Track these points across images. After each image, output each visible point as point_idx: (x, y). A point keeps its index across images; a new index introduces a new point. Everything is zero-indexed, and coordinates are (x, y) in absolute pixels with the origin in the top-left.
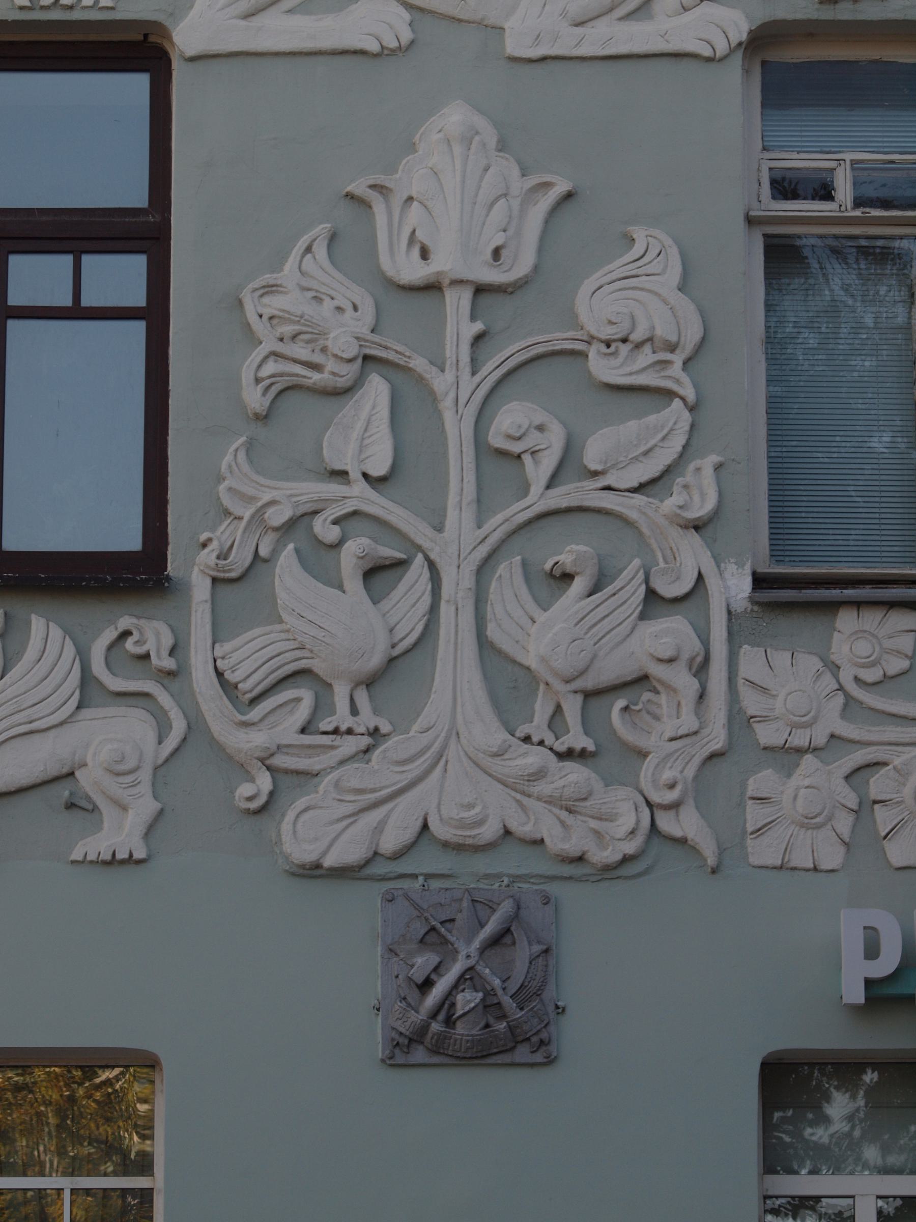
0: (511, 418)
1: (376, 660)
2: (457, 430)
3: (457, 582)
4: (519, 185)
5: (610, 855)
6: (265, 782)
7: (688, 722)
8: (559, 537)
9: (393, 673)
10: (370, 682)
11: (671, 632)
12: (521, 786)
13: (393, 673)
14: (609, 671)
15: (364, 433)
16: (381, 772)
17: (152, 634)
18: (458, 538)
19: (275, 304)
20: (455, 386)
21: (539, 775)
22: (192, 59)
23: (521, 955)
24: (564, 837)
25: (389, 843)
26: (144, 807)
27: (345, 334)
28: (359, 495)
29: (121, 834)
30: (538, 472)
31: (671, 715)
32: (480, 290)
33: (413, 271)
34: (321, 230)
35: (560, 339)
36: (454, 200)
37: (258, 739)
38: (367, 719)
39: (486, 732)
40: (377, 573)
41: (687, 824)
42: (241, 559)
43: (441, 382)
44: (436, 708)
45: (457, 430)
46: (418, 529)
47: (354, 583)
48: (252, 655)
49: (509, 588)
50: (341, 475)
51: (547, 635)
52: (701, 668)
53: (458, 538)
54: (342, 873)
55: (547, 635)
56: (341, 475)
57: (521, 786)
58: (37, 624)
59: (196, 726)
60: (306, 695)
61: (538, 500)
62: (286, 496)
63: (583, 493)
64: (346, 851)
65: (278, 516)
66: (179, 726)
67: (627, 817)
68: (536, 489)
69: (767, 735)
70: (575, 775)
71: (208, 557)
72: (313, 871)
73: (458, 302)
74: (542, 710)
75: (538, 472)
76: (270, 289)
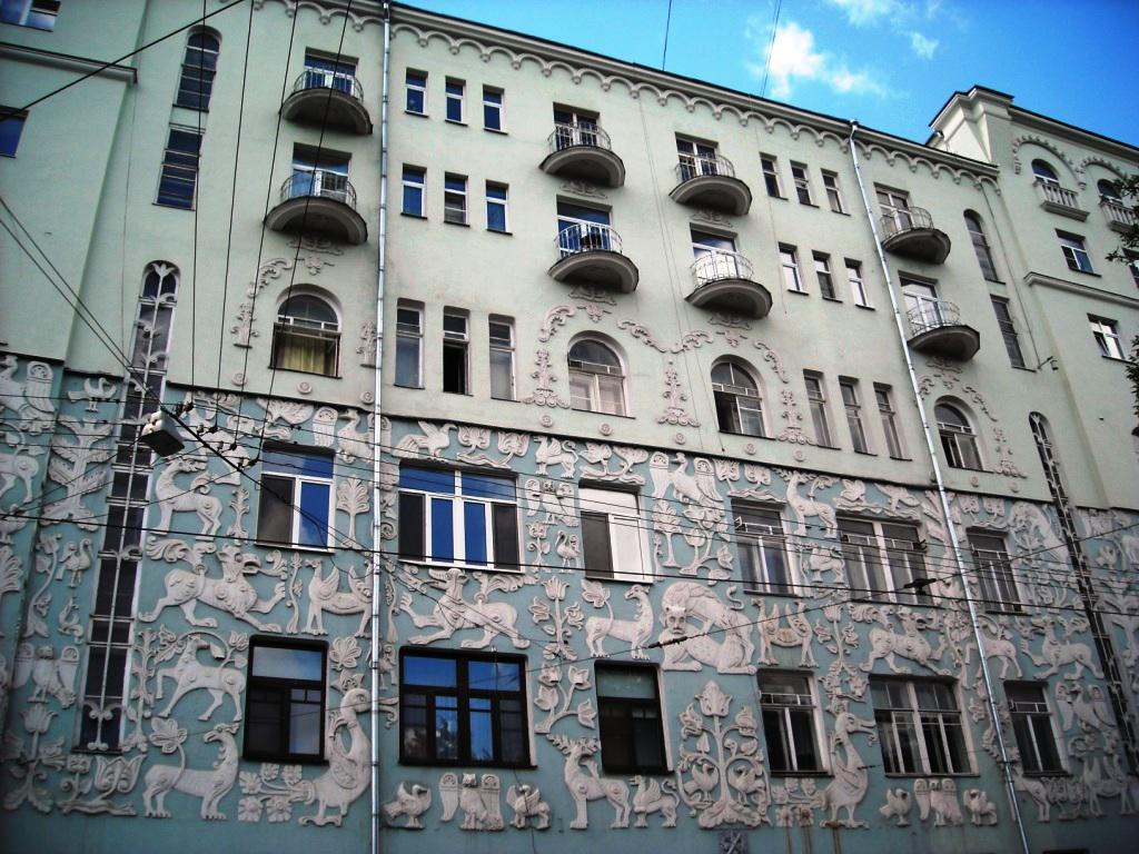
0: (728, 741)
1: (711, 788)
2: (719, 743)
3: (723, 773)
4: (724, 697)
5: (755, 825)
6: (694, 812)
7: (764, 799)
8: (739, 765)
9: (714, 790)
10: (710, 792)
11: (759, 783)
12: (739, 812)
13: (714, 790)
14: (751, 789)
15: (703, 743)
16: (714, 809)
17: (671, 783)
18: (722, 764)
19: (686, 718)
20: (718, 735)
21: (742, 810)
22: (666, 671)
23: (742, 844)
24: (747, 822)
25: (718, 823)
26: (674, 816)
27: (699, 725)
28: (705, 756)
29: (670, 821)
30: (734, 751)
31: (761, 799)
32: (720, 717)
33: (708, 713)
34: (691, 705)
35: (733, 726)
36: (714, 702)
37: (692, 803)
38: (711, 799)
39: (732, 801)
40: (710, 771)
41: (767, 819)
42: (685, 767)
43: (715, 734)
44: (722, 798)
45: (719, 743)
46: (715, 762)
47: (706, 773)
48: (691, 786)
49: (731, 773)
50: (700, 752)
51: (740, 782)
52: (765, 789)
53: (722, 764)
54: (711, 829)
55: (740, 782)
56: (700, 752)
57: (739, 812)
58: (652, 780)
59: (681, 801)
60: (700, 794)
61: (734, 757)
62: (692, 756)
63: (740, 756)
64: (711, 824)
65: (692, 759)
66: (678, 800)
67: (758, 818)
68: (734, 755)
69: (778, 802)
70: (747, 810)
71: (680, 767)
72: (705, 829)
73: (716, 719)
74: (739, 797)
75: (734, 751)
76: (685, 716)
